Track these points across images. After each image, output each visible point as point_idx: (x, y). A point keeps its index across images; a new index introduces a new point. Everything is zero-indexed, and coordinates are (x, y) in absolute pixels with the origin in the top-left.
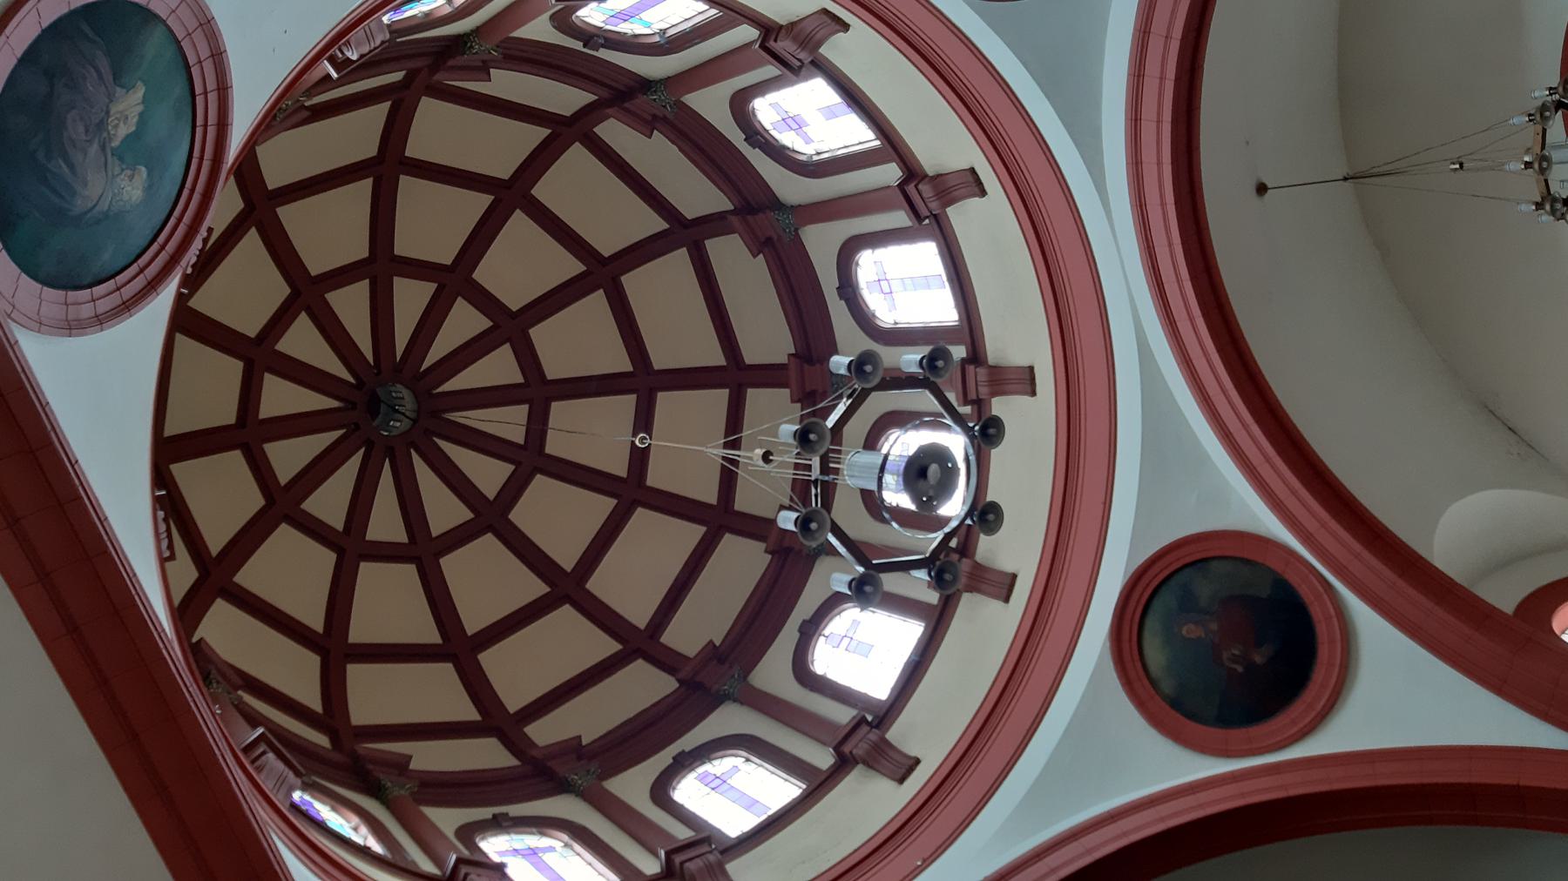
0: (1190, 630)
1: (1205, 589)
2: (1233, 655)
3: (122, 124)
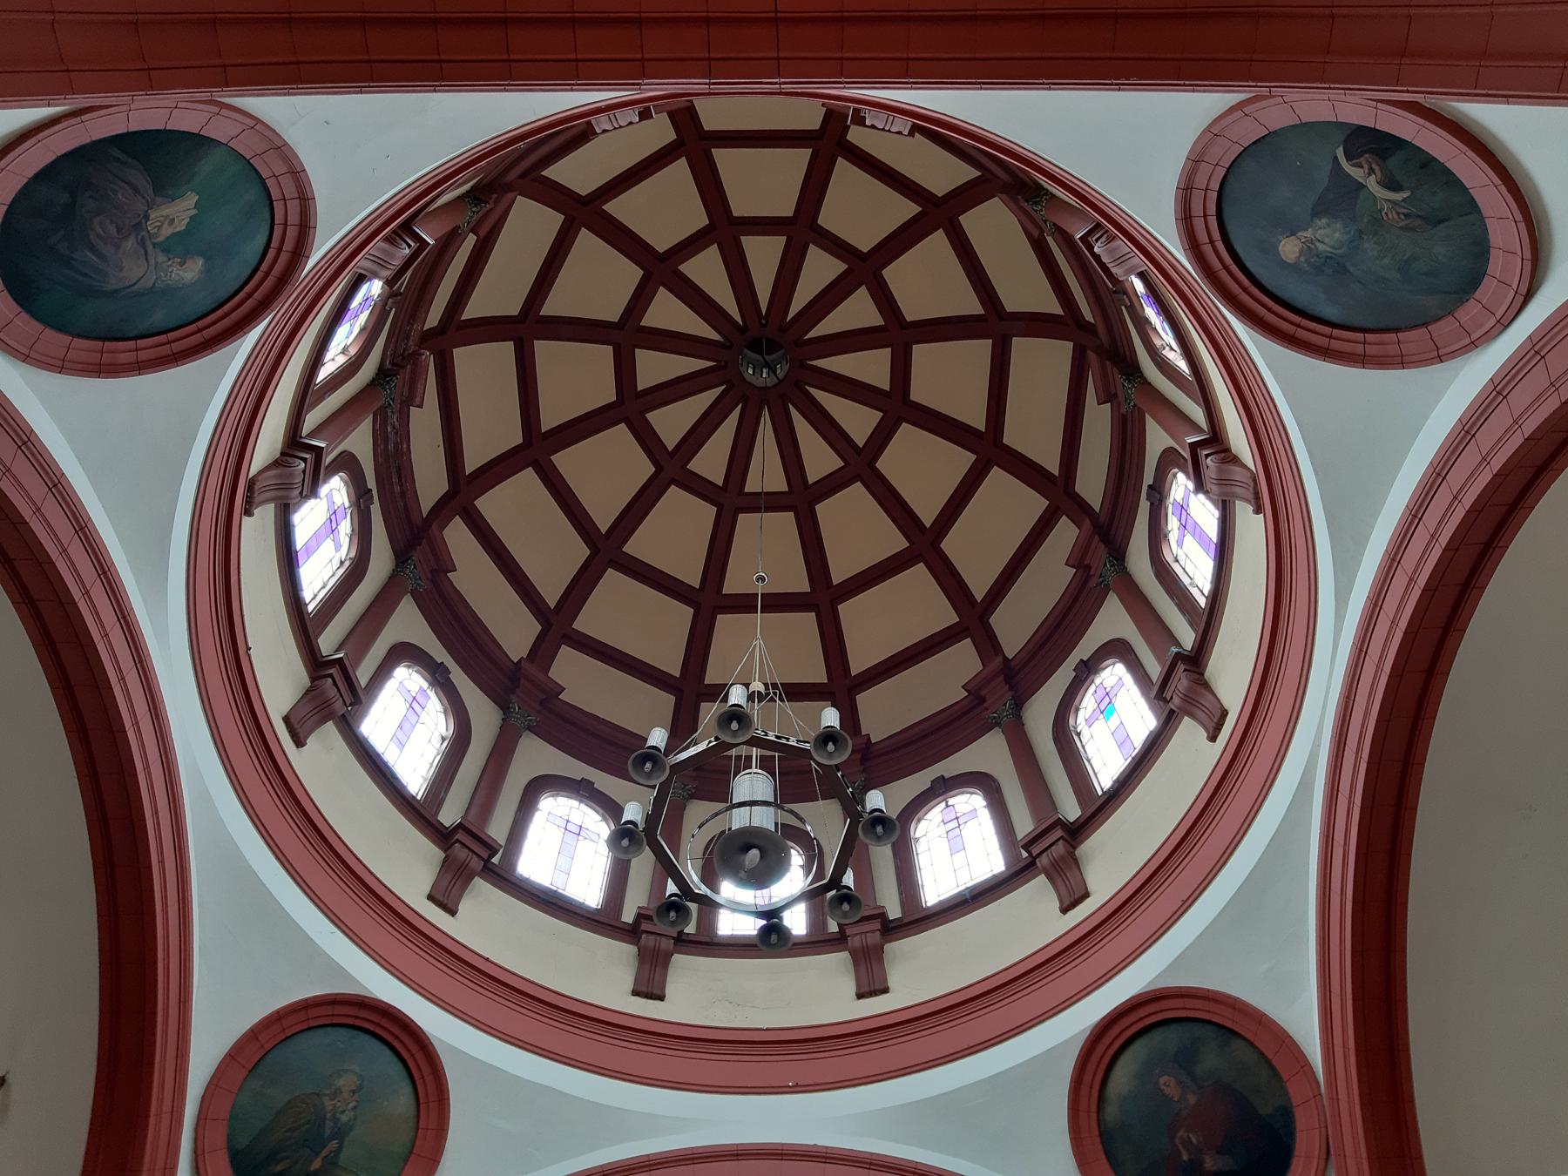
0: (1168, 1084)
1: (1210, 1060)
3: (166, 225)
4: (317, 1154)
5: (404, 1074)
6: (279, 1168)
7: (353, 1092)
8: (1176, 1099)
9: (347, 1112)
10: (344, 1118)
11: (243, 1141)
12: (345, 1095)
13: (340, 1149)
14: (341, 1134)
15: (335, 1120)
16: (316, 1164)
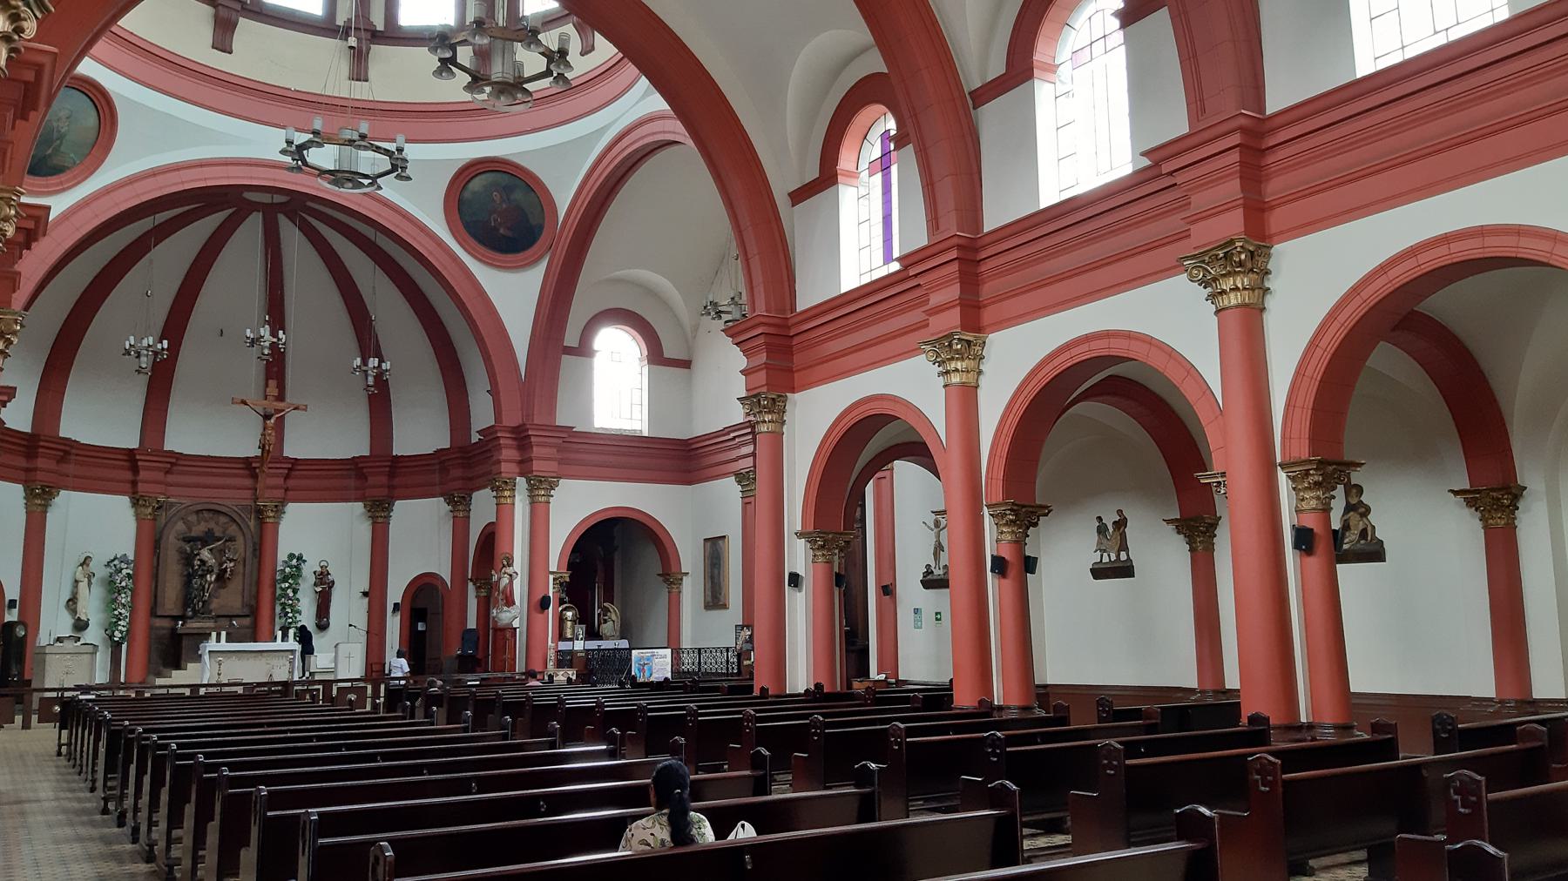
1: (518, 196)
10: (63, 130)
13: (61, 143)
14: (61, 137)
16: (50, 151)
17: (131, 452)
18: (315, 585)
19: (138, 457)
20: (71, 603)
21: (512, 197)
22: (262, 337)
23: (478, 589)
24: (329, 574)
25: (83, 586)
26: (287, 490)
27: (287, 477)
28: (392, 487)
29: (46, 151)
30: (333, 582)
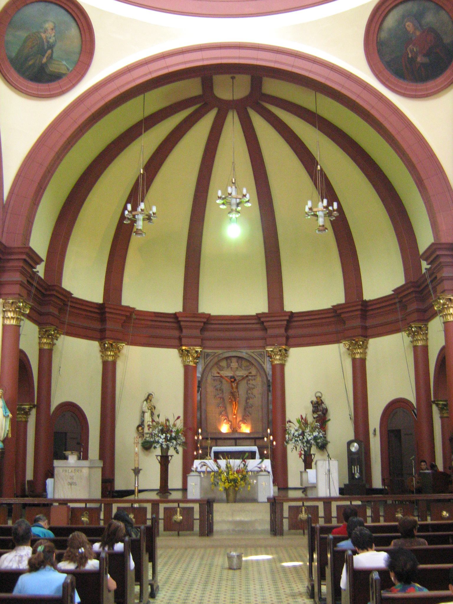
0: (409, 26)
1: (430, 18)
2: (413, 49)
4: (44, 56)
5: (72, 19)
6: (31, 63)
7: (52, 29)
8: (411, 32)
9: (52, 38)
10: (51, 41)
11: (14, 54)
12: (50, 31)
14: (51, 47)
15: (48, 42)
17: (175, 316)
18: (314, 412)
19: (180, 319)
20: (140, 428)
21: (423, 22)
22: (230, 194)
23: (441, 410)
24: (322, 403)
25: (147, 416)
26: (288, 338)
27: (287, 328)
28: (365, 328)
29: (41, 59)
30: (326, 410)
